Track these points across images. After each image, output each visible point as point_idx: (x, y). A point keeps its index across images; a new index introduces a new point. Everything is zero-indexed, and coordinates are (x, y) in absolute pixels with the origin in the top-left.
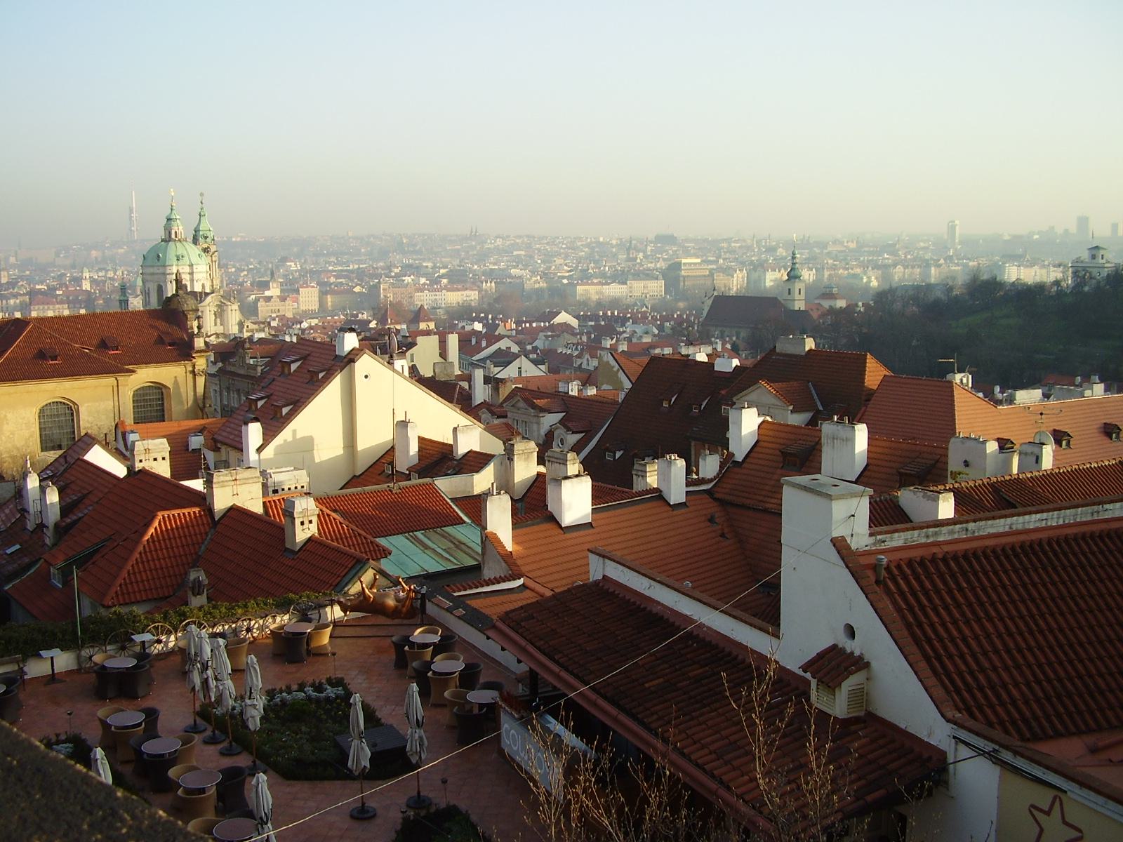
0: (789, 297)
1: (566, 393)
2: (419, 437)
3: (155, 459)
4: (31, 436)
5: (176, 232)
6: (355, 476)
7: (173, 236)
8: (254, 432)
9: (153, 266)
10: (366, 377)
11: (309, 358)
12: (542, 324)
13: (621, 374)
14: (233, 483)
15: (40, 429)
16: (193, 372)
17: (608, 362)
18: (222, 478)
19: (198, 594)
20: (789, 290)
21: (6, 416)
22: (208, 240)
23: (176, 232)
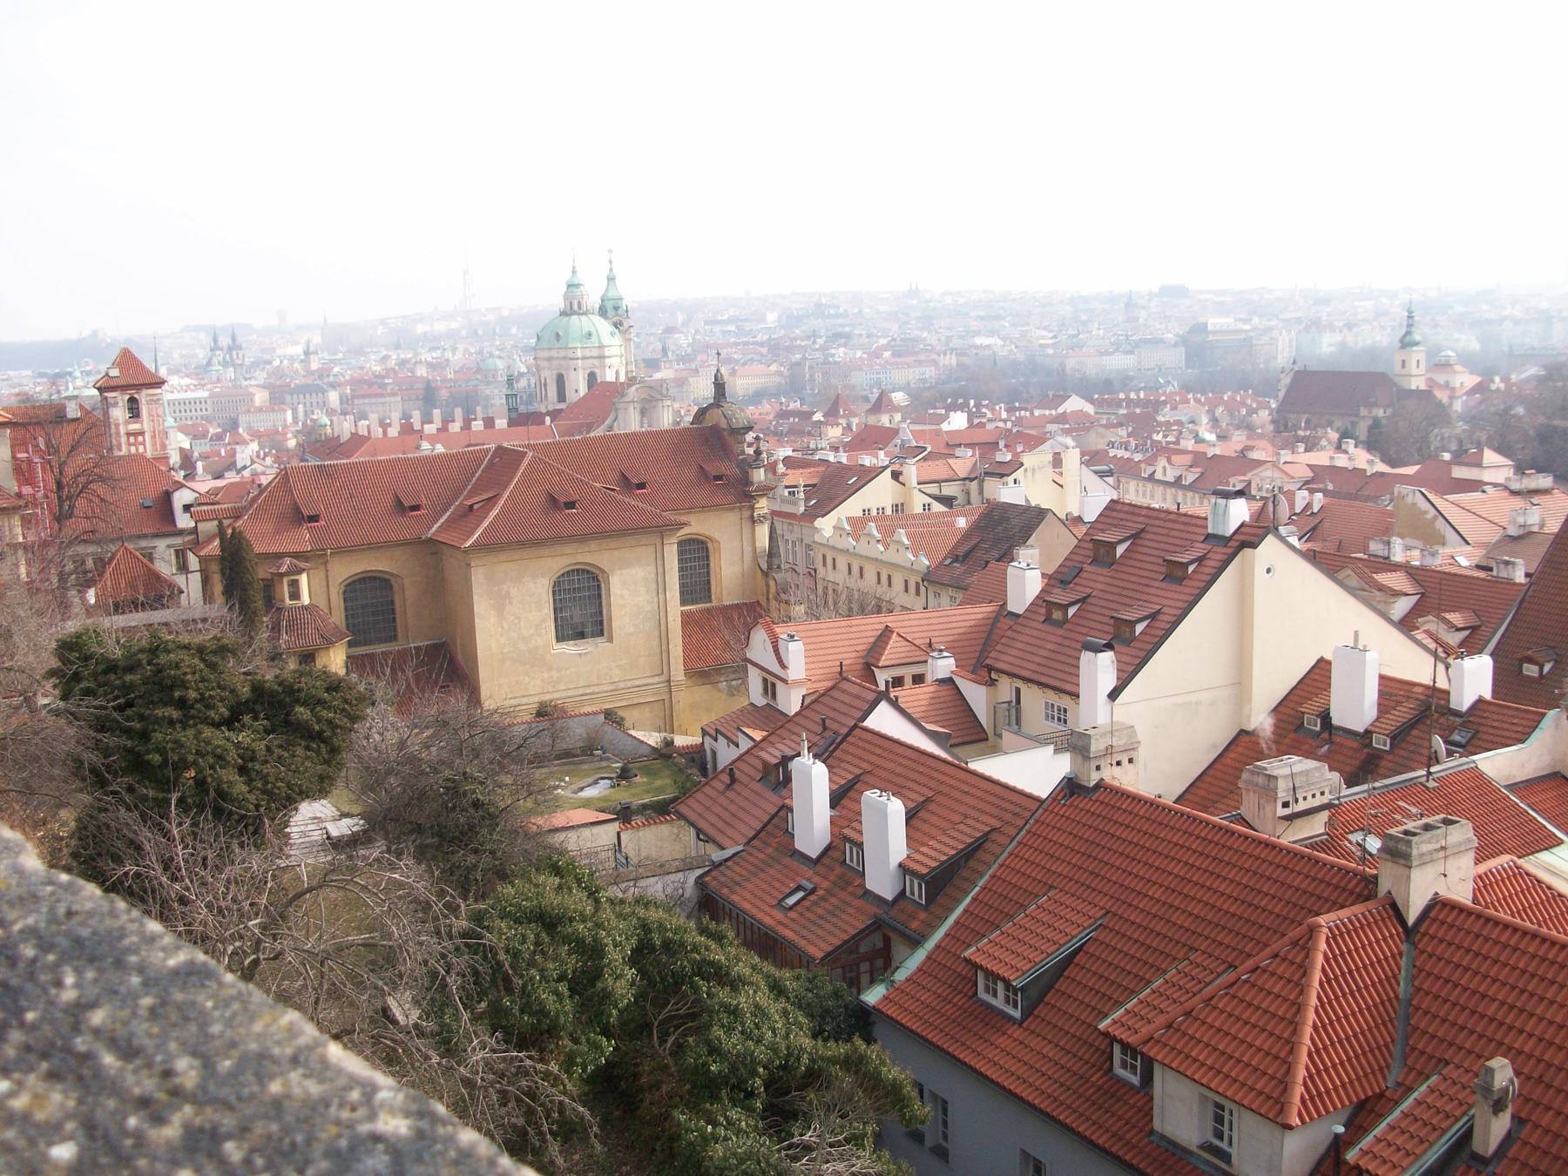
0: (1404, 372)
1: (1385, 558)
2: (1382, 678)
3: (1118, 763)
4: (544, 620)
5: (579, 303)
6: (1242, 731)
7: (576, 307)
8: (1100, 669)
9: (549, 349)
10: (1268, 571)
11: (1143, 535)
12: (1047, 412)
13: (1440, 523)
14: (1442, 854)
15: (555, 610)
16: (753, 521)
17: (1414, 504)
18: (1425, 848)
19: (1502, 1110)
20: (1404, 362)
21: (508, 593)
22: (620, 312)
23: (579, 303)
